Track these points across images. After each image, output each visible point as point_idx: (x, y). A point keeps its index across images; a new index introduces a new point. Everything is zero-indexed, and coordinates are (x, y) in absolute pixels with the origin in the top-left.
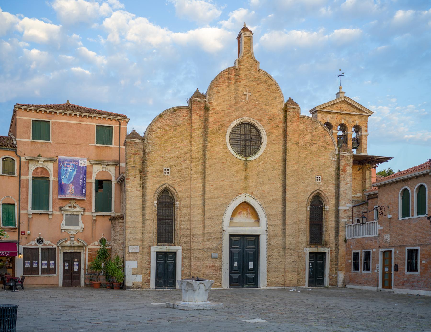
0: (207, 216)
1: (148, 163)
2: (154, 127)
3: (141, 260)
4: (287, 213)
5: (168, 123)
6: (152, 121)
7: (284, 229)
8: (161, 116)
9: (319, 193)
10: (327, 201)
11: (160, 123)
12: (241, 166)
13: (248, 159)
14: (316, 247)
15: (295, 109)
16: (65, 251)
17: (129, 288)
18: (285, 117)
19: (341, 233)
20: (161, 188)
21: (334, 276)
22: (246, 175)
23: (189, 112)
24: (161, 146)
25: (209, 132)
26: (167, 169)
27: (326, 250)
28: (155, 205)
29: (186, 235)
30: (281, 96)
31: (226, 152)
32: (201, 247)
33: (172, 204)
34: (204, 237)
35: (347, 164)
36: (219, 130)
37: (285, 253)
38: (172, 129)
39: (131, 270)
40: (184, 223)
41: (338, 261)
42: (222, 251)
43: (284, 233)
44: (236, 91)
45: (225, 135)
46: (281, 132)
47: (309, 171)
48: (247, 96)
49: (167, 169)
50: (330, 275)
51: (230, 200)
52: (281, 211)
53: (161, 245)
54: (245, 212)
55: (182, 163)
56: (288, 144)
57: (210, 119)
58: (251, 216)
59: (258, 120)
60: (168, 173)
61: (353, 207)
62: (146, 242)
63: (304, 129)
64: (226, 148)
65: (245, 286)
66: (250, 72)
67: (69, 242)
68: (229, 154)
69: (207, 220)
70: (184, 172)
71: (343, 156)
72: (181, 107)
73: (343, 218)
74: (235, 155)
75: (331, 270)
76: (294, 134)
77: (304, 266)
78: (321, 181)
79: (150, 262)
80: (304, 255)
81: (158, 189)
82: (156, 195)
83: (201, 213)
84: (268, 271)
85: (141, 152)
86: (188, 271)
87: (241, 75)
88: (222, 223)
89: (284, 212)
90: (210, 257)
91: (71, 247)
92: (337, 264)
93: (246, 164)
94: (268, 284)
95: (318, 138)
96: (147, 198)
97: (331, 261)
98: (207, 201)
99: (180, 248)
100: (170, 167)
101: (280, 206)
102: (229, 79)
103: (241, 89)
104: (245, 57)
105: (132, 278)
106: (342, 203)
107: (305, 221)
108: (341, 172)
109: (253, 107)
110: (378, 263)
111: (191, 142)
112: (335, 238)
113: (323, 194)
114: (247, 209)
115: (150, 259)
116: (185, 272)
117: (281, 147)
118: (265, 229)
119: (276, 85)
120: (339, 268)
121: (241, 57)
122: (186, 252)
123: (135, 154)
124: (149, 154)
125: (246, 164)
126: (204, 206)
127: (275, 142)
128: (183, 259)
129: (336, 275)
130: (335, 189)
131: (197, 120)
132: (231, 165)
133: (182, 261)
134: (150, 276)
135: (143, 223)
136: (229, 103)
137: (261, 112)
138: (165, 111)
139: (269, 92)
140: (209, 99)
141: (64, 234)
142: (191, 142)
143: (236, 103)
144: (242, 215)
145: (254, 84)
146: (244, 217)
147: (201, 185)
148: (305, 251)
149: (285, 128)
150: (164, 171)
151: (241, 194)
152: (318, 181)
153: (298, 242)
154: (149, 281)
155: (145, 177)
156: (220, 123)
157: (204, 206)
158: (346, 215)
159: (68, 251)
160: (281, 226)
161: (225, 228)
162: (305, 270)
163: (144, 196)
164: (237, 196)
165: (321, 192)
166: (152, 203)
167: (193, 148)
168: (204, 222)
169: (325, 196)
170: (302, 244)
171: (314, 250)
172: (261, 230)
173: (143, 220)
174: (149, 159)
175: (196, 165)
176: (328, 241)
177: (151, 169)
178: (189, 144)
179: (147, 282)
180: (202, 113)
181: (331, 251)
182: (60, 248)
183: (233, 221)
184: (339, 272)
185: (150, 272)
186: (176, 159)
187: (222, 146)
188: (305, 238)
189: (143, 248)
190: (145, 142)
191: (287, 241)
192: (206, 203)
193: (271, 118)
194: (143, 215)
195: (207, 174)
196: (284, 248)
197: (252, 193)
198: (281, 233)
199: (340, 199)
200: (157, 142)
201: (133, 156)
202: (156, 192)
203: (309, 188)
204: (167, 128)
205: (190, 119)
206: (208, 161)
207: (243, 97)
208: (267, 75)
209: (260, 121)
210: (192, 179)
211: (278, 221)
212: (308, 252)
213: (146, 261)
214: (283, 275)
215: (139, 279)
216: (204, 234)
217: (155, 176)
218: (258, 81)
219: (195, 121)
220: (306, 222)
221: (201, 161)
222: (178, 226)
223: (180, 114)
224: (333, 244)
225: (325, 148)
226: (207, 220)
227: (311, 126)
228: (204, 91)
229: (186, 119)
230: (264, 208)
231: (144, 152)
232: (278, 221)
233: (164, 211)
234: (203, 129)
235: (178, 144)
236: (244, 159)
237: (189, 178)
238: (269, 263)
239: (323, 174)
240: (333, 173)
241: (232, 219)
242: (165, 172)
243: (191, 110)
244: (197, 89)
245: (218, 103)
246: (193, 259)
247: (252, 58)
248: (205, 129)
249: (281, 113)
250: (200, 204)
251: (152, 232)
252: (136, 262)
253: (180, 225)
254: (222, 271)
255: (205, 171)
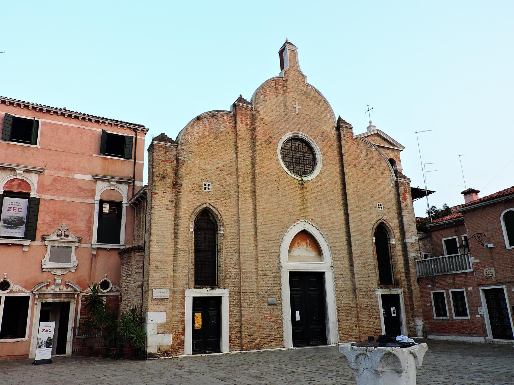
0: (260, 247)
1: (182, 174)
2: (190, 131)
3: (171, 311)
4: (352, 245)
5: (208, 129)
6: (188, 124)
7: (352, 265)
8: (198, 118)
9: (382, 223)
10: (392, 232)
11: (197, 127)
12: (297, 186)
13: (304, 179)
14: (387, 287)
15: (348, 128)
16: (44, 301)
17: (152, 356)
18: (339, 136)
19: (412, 271)
20: (200, 208)
21: (412, 324)
22: (303, 197)
23: (233, 118)
24: (199, 155)
25: (257, 144)
26: (207, 184)
27: (398, 291)
28: (192, 230)
29: (233, 272)
30: (332, 114)
31: (279, 169)
32: (255, 289)
33: (215, 230)
34: (257, 276)
35: (406, 192)
36: (269, 143)
37: (355, 296)
38: (213, 136)
39: (156, 326)
40: (231, 256)
41: (413, 305)
42: (281, 295)
43: (352, 270)
44: (285, 102)
45: (277, 149)
46: (335, 151)
47: (369, 197)
48: (297, 109)
49: (207, 184)
50: (408, 323)
51: (287, 227)
52: (345, 242)
53: (200, 288)
54: (304, 243)
55: (227, 178)
56: (345, 165)
57: (258, 129)
58: (311, 249)
59: (311, 136)
60: (209, 189)
61: (419, 240)
62: (178, 283)
63: (359, 151)
64: (279, 164)
65: (311, 344)
66: (298, 86)
67: (53, 287)
68: (283, 171)
69: (261, 252)
70: (229, 189)
71: (402, 183)
72: (223, 111)
73: (411, 252)
74: (289, 172)
75: (407, 317)
76: (350, 155)
77: (378, 312)
78: (382, 209)
79: (183, 314)
80: (376, 298)
81: (196, 209)
82: (193, 217)
83: (253, 243)
84: (339, 321)
85: (173, 158)
86: (238, 324)
87: (288, 87)
88: (279, 256)
89: (349, 244)
90: (266, 304)
91: (54, 295)
92: (412, 309)
93: (302, 184)
94: (340, 339)
95: (374, 162)
96: (181, 221)
97: (405, 305)
98: (259, 227)
99: (226, 291)
100: (211, 181)
101: (344, 236)
102: (276, 89)
103: (289, 100)
104: (291, 70)
105: (155, 340)
106: (407, 234)
107: (372, 255)
108: (402, 200)
109: (304, 121)
110: (481, 305)
111: (236, 153)
112: (406, 277)
113: (387, 224)
114: (306, 240)
115: (184, 308)
116: (234, 326)
117: (338, 168)
118: (330, 265)
119: (326, 101)
120: (416, 314)
121: (286, 68)
122: (235, 296)
123: (165, 161)
124: (183, 163)
125: (303, 184)
126: (256, 233)
127: (331, 162)
128: (230, 307)
129: (413, 324)
130: (398, 219)
131: (243, 127)
132: (285, 185)
133: (230, 311)
134: (183, 334)
135: (175, 256)
136: (278, 113)
137: (313, 128)
138: (205, 113)
139: (319, 108)
140: (255, 107)
141: (45, 275)
142: (236, 153)
143: (286, 115)
144: (301, 247)
145: (303, 97)
146: (304, 250)
147: (252, 206)
148: (377, 293)
149: (340, 147)
150: (204, 187)
151: (298, 220)
152: (380, 209)
153: (369, 281)
154: (182, 344)
155: (177, 192)
156: (270, 135)
157: (256, 233)
158: (414, 249)
159: (50, 300)
160: (347, 262)
161: (283, 264)
162: (380, 318)
163: (176, 217)
164: (294, 222)
165: (385, 222)
166: (187, 228)
167: (239, 160)
168: (256, 256)
169: (389, 227)
170: (372, 284)
171: (386, 291)
172: (324, 265)
173: (176, 250)
174: (183, 170)
175: (244, 181)
176: (400, 280)
177: (185, 182)
178: (234, 155)
179: (179, 344)
180: (249, 121)
181: (404, 292)
182: (37, 296)
183: (291, 254)
184: (417, 318)
185: (183, 329)
186: (219, 172)
187: (274, 162)
188: (374, 277)
189: (174, 292)
190: (179, 147)
191: (356, 280)
192: (258, 230)
193: (324, 135)
194: (176, 243)
195: (257, 194)
196: (354, 289)
197: (312, 220)
198: (348, 271)
199: (405, 230)
200: (195, 150)
201: (162, 164)
202: (193, 212)
203: (371, 216)
204: (206, 133)
205: (235, 126)
206: (258, 178)
207: (292, 109)
208: (316, 90)
209: (313, 137)
210: (240, 198)
211: (343, 255)
212: (381, 293)
213: (178, 312)
214: (356, 326)
215: (167, 340)
216: (257, 270)
217: (192, 192)
218: (306, 94)
219: (241, 129)
220: (374, 257)
221: (250, 176)
222: (223, 260)
223: (222, 119)
224: (405, 284)
225: (382, 173)
226: (261, 252)
227: (366, 148)
228: (248, 97)
229: (229, 126)
230: (326, 238)
231: (177, 160)
232: (343, 255)
233: (202, 240)
234: (251, 139)
235: (221, 154)
236: (299, 179)
237: (236, 198)
238: (339, 311)
239: (383, 201)
240: (394, 201)
241: (289, 252)
242: (205, 188)
243: (235, 116)
244: (240, 95)
245: (267, 111)
246: (245, 307)
247: (299, 71)
248: (253, 139)
249: (334, 132)
250: (252, 231)
251: (187, 268)
252: (164, 313)
253: (226, 258)
254: (282, 323)
255: (255, 189)
